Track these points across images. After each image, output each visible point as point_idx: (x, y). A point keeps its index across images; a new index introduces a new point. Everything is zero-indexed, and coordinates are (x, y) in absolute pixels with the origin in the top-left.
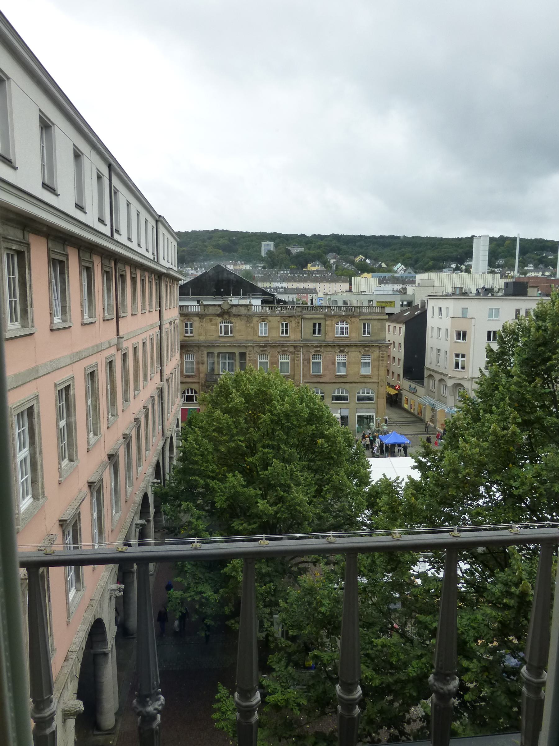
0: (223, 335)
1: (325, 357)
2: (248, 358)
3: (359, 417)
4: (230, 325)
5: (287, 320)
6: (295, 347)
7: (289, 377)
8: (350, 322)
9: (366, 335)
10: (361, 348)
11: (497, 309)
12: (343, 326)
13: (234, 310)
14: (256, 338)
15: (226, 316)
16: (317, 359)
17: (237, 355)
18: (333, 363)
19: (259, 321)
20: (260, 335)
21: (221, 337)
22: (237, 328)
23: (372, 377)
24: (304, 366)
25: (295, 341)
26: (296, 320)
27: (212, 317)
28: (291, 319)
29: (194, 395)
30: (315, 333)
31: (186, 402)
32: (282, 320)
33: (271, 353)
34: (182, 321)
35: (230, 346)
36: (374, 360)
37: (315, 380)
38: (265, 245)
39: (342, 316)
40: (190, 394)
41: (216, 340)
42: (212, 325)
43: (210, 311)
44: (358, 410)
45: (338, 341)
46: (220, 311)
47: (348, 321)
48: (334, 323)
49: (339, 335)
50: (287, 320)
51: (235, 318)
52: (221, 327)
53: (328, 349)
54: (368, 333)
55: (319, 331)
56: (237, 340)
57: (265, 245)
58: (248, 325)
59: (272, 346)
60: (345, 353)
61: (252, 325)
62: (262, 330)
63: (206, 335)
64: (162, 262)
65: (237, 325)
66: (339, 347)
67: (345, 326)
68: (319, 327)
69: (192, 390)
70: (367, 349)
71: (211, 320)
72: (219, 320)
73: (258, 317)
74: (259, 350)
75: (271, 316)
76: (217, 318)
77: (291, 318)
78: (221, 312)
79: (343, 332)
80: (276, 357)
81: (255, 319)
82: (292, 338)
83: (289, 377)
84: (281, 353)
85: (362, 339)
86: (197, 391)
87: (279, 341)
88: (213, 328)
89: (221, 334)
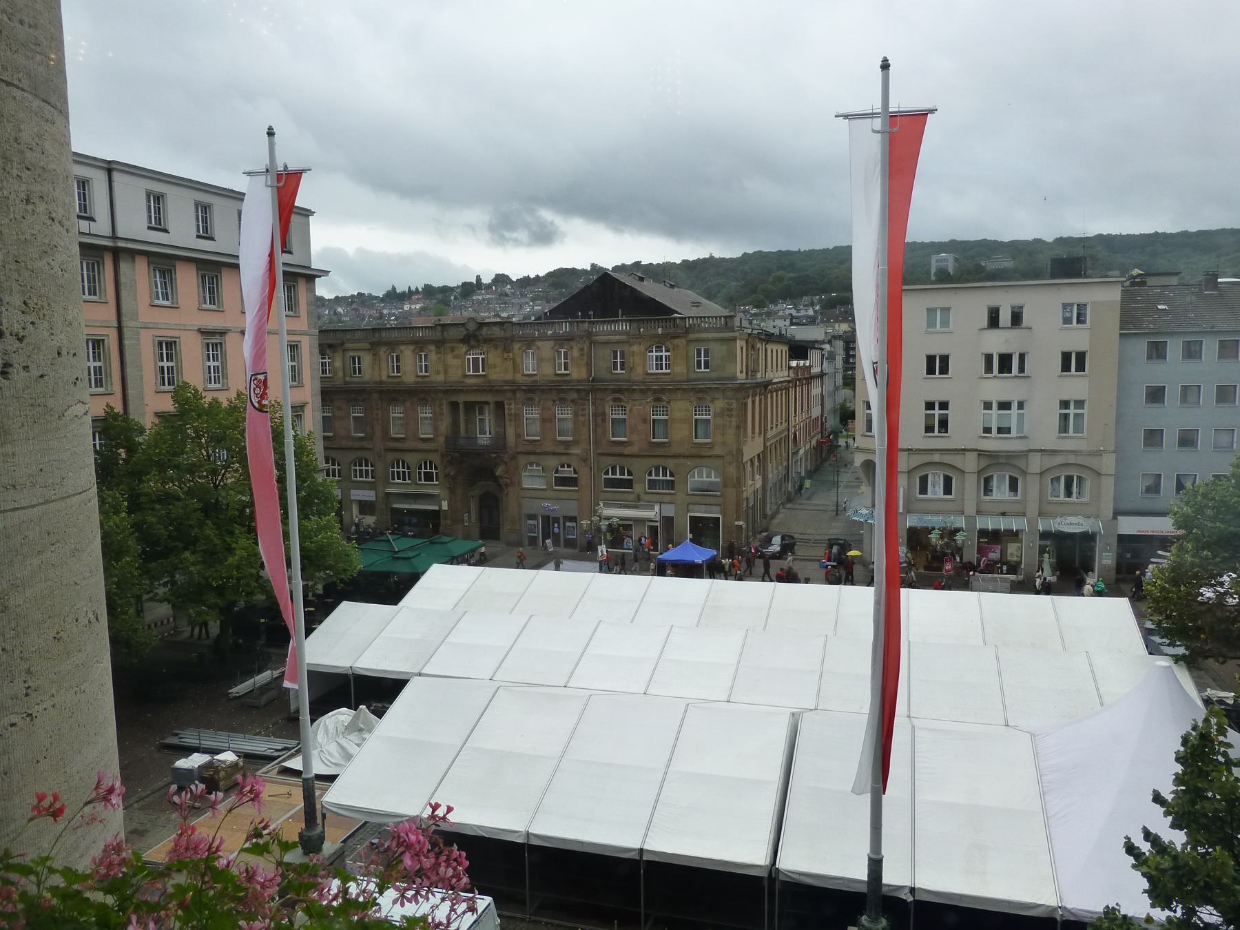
0: (471, 373)
2: (506, 412)
3: (694, 520)
4: (481, 357)
5: (565, 346)
6: (578, 391)
7: (572, 443)
8: (671, 347)
9: (703, 370)
10: (691, 394)
11: (946, 310)
12: (661, 354)
14: (519, 377)
15: (473, 342)
16: (619, 414)
18: (645, 421)
20: (525, 373)
22: (491, 361)
23: (670, 446)
24: (596, 426)
25: (579, 381)
26: (579, 345)
27: (453, 345)
29: (433, 471)
30: (615, 368)
32: (557, 347)
33: (542, 402)
35: (478, 391)
36: (715, 415)
37: (616, 449)
38: (937, 261)
39: (657, 336)
40: (428, 470)
41: (460, 382)
42: (454, 357)
43: (451, 334)
44: (691, 507)
46: (465, 332)
47: (668, 344)
48: (642, 348)
49: (654, 371)
50: (565, 346)
51: (486, 345)
53: (636, 396)
54: (706, 367)
55: (622, 364)
57: (937, 261)
58: (506, 355)
59: (543, 391)
60: (664, 403)
61: (511, 355)
62: (530, 365)
63: (446, 373)
64: (120, 233)
65: (490, 356)
66: (655, 391)
67: (664, 354)
68: (622, 357)
69: (431, 463)
70: (701, 395)
72: (464, 348)
73: (519, 341)
75: (540, 338)
76: (461, 345)
77: (571, 343)
78: (465, 336)
79: (662, 365)
80: (550, 409)
81: (516, 346)
82: (575, 376)
84: (557, 402)
85: (693, 376)
86: (437, 465)
87: (553, 382)
88: (456, 362)
89: (469, 371)
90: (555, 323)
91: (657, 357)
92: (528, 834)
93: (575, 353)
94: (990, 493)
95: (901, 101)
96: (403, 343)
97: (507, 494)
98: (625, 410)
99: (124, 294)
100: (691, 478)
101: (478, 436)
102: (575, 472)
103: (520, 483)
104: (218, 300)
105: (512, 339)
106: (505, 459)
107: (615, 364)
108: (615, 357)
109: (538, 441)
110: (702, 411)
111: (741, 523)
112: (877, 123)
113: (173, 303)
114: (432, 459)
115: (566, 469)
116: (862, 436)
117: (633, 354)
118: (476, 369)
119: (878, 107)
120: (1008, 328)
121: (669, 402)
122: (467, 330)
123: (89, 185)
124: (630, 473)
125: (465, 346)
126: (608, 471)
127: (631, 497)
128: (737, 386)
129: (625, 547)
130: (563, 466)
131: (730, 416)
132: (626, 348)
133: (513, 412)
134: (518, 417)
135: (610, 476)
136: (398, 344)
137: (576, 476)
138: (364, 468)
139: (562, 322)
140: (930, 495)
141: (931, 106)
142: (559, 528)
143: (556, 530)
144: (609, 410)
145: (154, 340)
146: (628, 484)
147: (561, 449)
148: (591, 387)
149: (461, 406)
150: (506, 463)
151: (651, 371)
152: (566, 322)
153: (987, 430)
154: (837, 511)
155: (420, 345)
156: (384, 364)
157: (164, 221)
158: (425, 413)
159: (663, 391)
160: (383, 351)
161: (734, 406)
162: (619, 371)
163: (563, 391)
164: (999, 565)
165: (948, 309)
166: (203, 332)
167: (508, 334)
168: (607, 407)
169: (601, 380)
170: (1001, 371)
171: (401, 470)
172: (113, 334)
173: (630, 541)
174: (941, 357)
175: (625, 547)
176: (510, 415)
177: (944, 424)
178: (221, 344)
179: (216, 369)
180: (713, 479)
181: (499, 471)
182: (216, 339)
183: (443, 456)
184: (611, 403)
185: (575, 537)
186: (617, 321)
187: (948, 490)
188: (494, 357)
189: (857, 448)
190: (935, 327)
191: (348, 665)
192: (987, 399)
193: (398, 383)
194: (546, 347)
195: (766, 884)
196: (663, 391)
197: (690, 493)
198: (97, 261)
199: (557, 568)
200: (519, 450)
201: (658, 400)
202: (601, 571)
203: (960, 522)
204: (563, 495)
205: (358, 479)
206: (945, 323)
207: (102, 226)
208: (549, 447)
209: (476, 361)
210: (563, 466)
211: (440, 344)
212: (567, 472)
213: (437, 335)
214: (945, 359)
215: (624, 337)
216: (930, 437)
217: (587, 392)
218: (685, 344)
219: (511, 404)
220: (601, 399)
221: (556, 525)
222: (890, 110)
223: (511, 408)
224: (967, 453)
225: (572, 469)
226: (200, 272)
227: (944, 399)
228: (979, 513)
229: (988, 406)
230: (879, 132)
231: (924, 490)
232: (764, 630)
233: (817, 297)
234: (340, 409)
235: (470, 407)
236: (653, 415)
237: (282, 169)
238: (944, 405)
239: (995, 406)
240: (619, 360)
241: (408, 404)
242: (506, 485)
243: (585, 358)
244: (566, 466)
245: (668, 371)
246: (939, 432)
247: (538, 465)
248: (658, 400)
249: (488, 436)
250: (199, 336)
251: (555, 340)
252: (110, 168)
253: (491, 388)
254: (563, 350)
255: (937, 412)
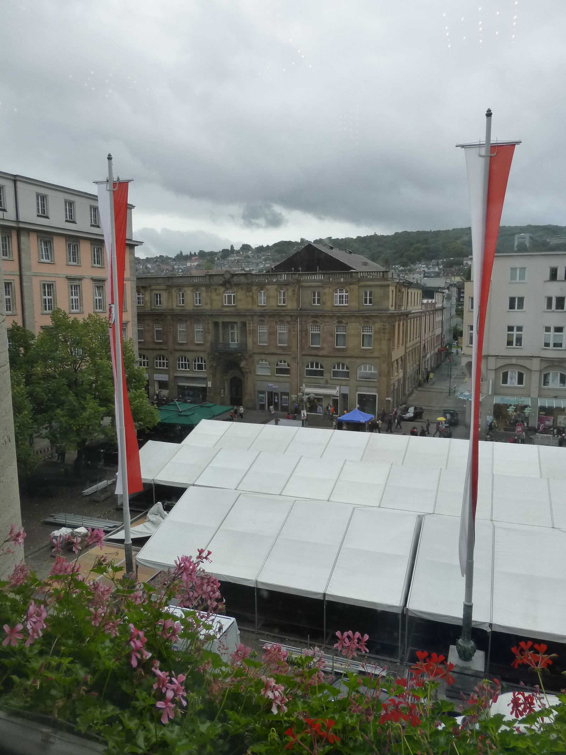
0: (227, 304)
1: (323, 329)
2: (248, 328)
4: (232, 295)
6: (291, 316)
7: (287, 348)
8: (348, 289)
10: (361, 319)
11: (523, 269)
13: (235, 279)
14: (256, 308)
15: (228, 286)
17: (239, 325)
18: (332, 335)
19: (258, 290)
20: (259, 304)
21: (225, 306)
24: (302, 337)
25: (292, 310)
26: (292, 288)
28: (288, 287)
29: (203, 363)
30: (314, 302)
31: (197, 370)
32: (279, 289)
33: (269, 323)
34: (192, 291)
36: (375, 332)
37: (313, 352)
40: (200, 363)
41: (221, 310)
42: (218, 295)
44: (359, 388)
45: (337, 310)
46: (224, 280)
48: (331, 290)
49: (338, 304)
52: (225, 296)
53: (327, 320)
54: (370, 302)
55: (319, 300)
56: (238, 310)
57: (519, 238)
58: (248, 294)
59: (270, 316)
60: (344, 325)
61: (251, 294)
62: (262, 299)
63: (211, 304)
65: (238, 293)
66: (338, 317)
67: (344, 294)
68: (319, 296)
69: (202, 359)
70: (366, 320)
71: (216, 290)
72: (222, 289)
73: (256, 285)
74: (256, 319)
75: (269, 284)
79: (343, 301)
81: (254, 288)
83: (287, 348)
85: (362, 308)
89: (225, 303)
90: (278, 274)
91: (340, 296)
92: (257, 582)
93: (290, 293)
94: (547, 384)
95: (498, 137)
96: (187, 286)
97: (247, 378)
98: (320, 328)
99: (23, 255)
100: (359, 370)
101: (230, 343)
102: (288, 366)
103: (255, 372)
104: (78, 259)
105: (252, 284)
106: (247, 358)
107: (314, 300)
108: (314, 296)
109: (266, 346)
110: (367, 329)
111: (390, 399)
112: (483, 152)
113: (51, 261)
114: (202, 357)
115: (283, 363)
116: (467, 346)
117: (325, 294)
118: (230, 302)
119: (483, 140)
120: (562, 281)
121: (347, 324)
122: (225, 278)
123: (3, 190)
124: (322, 367)
125: (223, 288)
126: (308, 365)
127: (322, 382)
128: (390, 314)
129: (318, 412)
130: (281, 362)
131: (384, 333)
132: (321, 290)
133: (251, 328)
134: (254, 332)
135: (310, 368)
136: (183, 287)
137: (289, 368)
138: (162, 361)
139: (282, 274)
140: (509, 384)
141: (517, 140)
142: (278, 399)
143: (276, 400)
144: (310, 328)
145: (40, 283)
146: (321, 373)
147: (280, 352)
148: (299, 314)
149: (220, 324)
150: (247, 359)
151: (336, 305)
152: (284, 274)
153: (547, 345)
154: (450, 392)
155: (196, 287)
156: (174, 298)
157: (47, 212)
158: (198, 328)
159: (343, 317)
160: (174, 291)
161: (387, 327)
162: (316, 304)
163: (282, 316)
164: (552, 429)
165: (525, 268)
166: (69, 279)
167: (249, 281)
168: (308, 326)
169: (306, 310)
170: (557, 308)
171: (184, 362)
172: (17, 279)
173: (321, 408)
174: (519, 298)
175: (318, 412)
176: (250, 330)
177: (519, 340)
178: (79, 285)
179: (76, 301)
180: (373, 371)
181: (243, 364)
182: (76, 283)
183: (209, 354)
184: (311, 324)
185: (287, 405)
186: (315, 274)
187: (520, 381)
188: (240, 294)
189: (464, 354)
190: (516, 279)
191: (152, 478)
192: (548, 325)
193: (182, 310)
194: (272, 289)
195: (400, 617)
196: (343, 317)
197: (358, 379)
198: (8, 236)
199: (277, 423)
200: (255, 352)
201: (340, 322)
202: (303, 426)
203: (528, 402)
204: (281, 379)
205: (158, 367)
206: (522, 277)
207: (10, 215)
208: (273, 350)
209: (229, 297)
210: (281, 362)
211: (208, 286)
212: (283, 365)
213: (207, 281)
214: (521, 300)
215: (320, 284)
216: (510, 348)
217: (297, 317)
218: (358, 288)
219: (250, 324)
220: (305, 321)
221: (276, 397)
222: (492, 142)
223: (250, 326)
224: (533, 359)
225: (287, 363)
226: (68, 243)
227: (520, 324)
228: (540, 396)
229: (548, 329)
230: (483, 156)
231: (505, 381)
232: (403, 464)
233: (441, 260)
234: (148, 325)
235: (225, 324)
236: (337, 331)
237: (116, 180)
238: (520, 329)
239: (552, 329)
240: (316, 298)
241: (189, 323)
242: (247, 373)
243: (296, 296)
244: (283, 362)
245: (347, 305)
246: (516, 345)
247: (266, 361)
248: (340, 322)
249: (236, 342)
250: (67, 280)
251: (278, 285)
252: (15, 179)
253: (239, 314)
254: (282, 291)
255: (515, 333)
